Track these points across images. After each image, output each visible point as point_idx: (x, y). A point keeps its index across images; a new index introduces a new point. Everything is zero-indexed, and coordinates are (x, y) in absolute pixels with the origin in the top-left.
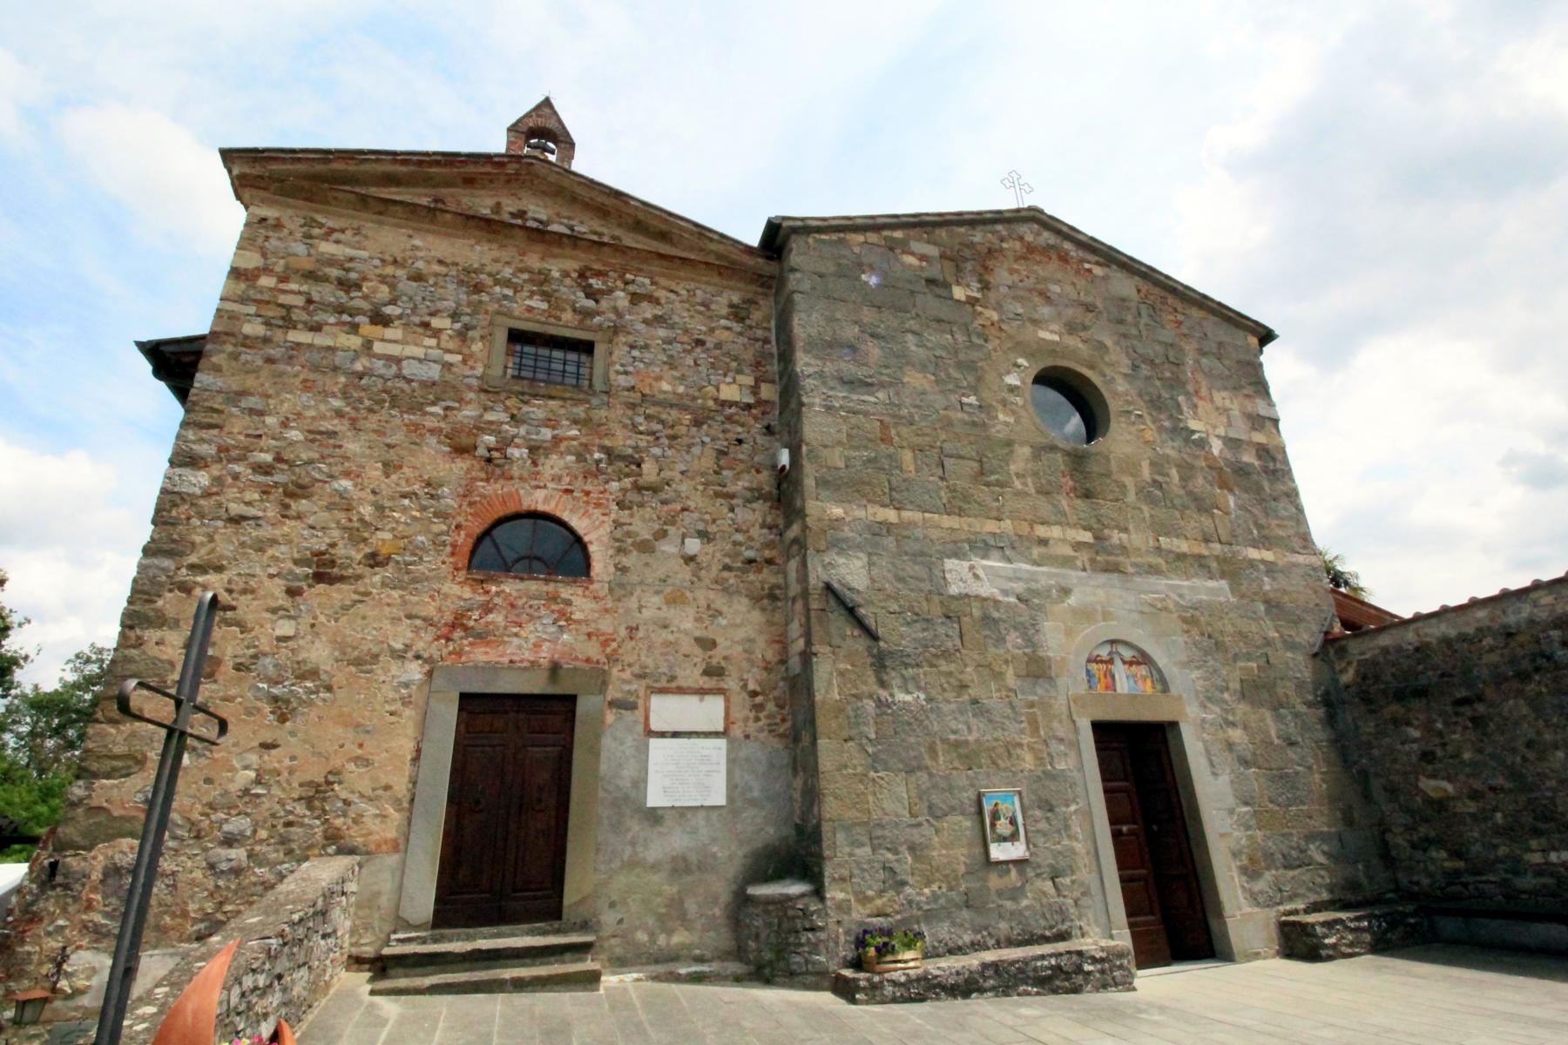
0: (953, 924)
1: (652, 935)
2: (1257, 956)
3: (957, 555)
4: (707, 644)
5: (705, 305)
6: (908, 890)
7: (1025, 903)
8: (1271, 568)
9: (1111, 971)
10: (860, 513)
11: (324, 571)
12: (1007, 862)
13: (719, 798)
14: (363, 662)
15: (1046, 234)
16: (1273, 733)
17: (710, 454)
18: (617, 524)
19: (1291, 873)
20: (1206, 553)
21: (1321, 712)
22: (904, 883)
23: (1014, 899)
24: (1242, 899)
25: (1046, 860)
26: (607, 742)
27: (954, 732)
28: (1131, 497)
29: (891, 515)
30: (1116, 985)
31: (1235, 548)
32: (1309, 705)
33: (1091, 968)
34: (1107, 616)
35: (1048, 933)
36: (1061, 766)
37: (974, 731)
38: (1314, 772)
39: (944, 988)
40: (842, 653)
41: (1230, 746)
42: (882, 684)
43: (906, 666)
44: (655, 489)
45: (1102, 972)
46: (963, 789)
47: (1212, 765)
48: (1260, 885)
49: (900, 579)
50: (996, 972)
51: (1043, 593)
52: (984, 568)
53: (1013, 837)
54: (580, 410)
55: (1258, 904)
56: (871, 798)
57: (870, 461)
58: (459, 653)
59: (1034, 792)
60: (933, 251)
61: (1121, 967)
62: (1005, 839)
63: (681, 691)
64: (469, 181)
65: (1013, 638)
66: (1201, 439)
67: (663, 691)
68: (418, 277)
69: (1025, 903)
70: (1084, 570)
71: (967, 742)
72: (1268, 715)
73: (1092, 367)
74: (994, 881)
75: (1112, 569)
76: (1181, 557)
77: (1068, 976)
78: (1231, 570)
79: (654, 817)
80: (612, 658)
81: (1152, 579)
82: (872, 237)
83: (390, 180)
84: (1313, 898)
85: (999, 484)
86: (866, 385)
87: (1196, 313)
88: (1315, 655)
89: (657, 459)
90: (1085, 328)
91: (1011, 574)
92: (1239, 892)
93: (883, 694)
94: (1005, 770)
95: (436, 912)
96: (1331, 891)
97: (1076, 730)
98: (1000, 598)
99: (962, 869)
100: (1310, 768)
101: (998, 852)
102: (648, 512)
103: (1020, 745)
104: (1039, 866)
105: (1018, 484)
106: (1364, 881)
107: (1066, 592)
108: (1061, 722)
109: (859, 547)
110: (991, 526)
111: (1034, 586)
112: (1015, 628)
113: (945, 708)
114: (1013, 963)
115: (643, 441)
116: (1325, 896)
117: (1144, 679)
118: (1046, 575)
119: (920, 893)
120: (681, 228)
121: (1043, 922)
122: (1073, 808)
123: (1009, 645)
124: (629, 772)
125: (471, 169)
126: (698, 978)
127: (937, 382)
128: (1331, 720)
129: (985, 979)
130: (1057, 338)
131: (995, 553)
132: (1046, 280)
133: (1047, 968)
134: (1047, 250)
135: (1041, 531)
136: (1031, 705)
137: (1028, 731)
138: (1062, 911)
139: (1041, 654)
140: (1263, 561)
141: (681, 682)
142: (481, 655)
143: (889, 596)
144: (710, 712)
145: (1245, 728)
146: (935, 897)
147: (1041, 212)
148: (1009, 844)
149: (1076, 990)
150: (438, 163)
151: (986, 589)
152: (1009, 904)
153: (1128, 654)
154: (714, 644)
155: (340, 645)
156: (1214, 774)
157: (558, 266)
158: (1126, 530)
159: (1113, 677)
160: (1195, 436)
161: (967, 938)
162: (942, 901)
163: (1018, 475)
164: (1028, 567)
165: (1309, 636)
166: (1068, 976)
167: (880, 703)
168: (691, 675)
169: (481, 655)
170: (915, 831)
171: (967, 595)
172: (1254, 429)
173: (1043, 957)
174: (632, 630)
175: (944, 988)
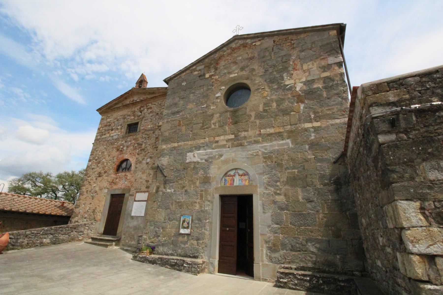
0: (168, 248)
1: (129, 241)
2: (265, 280)
3: (191, 151)
4: (147, 181)
5: (160, 105)
6: (160, 238)
7: (187, 246)
8: (316, 129)
9: (191, 268)
11: (100, 175)
12: (184, 234)
13: (143, 215)
14: (101, 189)
15: (240, 42)
16: (300, 198)
17: (154, 139)
18: (137, 158)
19: (294, 253)
21: (332, 187)
22: (159, 236)
23: (185, 244)
24: (265, 258)
25: (195, 235)
26: (128, 202)
27: (179, 199)
28: (253, 119)
29: (176, 145)
30: (192, 272)
31: (297, 125)
32: (325, 185)
33: (186, 265)
34: (234, 161)
35: (191, 255)
36: (207, 208)
37: (183, 198)
38: (320, 213)
39: (148, 261)
40: (158, 181)
41: (274, 202)
42: (165, 188)
43: (171, 183)
44: (144, 150)
45: (189, 267)
46: (178, 214)
47: (264, 208)
48: (277, 255)
50: (161, 260)
52: (197, 153)
53: (188, 228)
54: (135, 137)
55: (272, 262)
56: (156, 215)
57: (174, 132)
58: (112, 187)
59: (196, 215)
60: (202, 67)
61: (194, 267)
62: (185, 228)
63: (141, 192)
64: (126, 98)
65: (201, 172)
66: (291, 87)
67: (138, 192)
68: (118, 120)
69: (187, 246)
70: (229, 147)
71: (181, 202)
72: (299, 190)
73: (247, 79)
74: (180, 239)
75: (241, 145)
76: (270, 135)
78: (291, 134)
79: (132, 217)
80: (132, 186)
81: (255, 145)
82: (188, 72)
83: (116, 104)
84: (302, 265)
85: (207, 128)
86: (178, 112)
87: (302, 36)
88: (335, 163)
89: (145, 143)
90: (247, 66)
91: (204, 154)
92: (264, 256)
93: (164, 190)
94: (190, 209)
95: (104, 232)
96: (315, 264)
97: (214, 198)
98: (200, 161)
99: (173, 234)
100: (317, 211)
101: (182, 231)
102: (142, 155)
103: (196, 202)
104: (193, 237)
105: (213, 126)
106: (339, 264)
107: (221, 156)
108: (210, 195)
109: (167, 154)
110: (202, 141)
111: (211, 156)
112: (202, 169)
113: (178, 193)
114: (166, 259)
115: (143, 140)
116: (310, 265)
117: (246, 180)
118: (215, 152)
119: (162, 239)
120: (155, 90)
121: (190, 252)
122: (207, 221)
123: (199, 175)
124: (130, 209)
125: (125, 96)
126: (127, 250)
127: (196, 104)
128: (337, 190)
129: (158, 261)
130: (236, 75)
131: (202, 149)
132: (236, 57)
133: (174, 262)
134: (239, 48)
135: (217, 139)
136: (202, 191)
137: (199, 199)
138: (197, 250)
139: (208, 176)
140: (313, 127)
141: (142, 190)
142: (115, 187)
143: (171, 166)
144: (144, 196)
145: (285, 195)
146: (165, 241)
147: (237, 36)
148: (186, 229)
149: (180, 270)
150: (120, 98)
151: (196, 159)
152: (183, 246)
153: (241, 172)
154: (149, 181)
155: (100, 187)
156: (264, 212)
157: (136, 109)
158: (247, 131)
159: (234, 181)
160: (288, 87)
161: (170, 252)
162: (167, 242)
163: (213, 124)
164: (210, 150)
165: (332, 155)
168: (144, 189)
169: (115, 187)
170: (164, 224)
171: (191, 162)
173: (173, 259)
174: (136, 180)
175: (148, 261)
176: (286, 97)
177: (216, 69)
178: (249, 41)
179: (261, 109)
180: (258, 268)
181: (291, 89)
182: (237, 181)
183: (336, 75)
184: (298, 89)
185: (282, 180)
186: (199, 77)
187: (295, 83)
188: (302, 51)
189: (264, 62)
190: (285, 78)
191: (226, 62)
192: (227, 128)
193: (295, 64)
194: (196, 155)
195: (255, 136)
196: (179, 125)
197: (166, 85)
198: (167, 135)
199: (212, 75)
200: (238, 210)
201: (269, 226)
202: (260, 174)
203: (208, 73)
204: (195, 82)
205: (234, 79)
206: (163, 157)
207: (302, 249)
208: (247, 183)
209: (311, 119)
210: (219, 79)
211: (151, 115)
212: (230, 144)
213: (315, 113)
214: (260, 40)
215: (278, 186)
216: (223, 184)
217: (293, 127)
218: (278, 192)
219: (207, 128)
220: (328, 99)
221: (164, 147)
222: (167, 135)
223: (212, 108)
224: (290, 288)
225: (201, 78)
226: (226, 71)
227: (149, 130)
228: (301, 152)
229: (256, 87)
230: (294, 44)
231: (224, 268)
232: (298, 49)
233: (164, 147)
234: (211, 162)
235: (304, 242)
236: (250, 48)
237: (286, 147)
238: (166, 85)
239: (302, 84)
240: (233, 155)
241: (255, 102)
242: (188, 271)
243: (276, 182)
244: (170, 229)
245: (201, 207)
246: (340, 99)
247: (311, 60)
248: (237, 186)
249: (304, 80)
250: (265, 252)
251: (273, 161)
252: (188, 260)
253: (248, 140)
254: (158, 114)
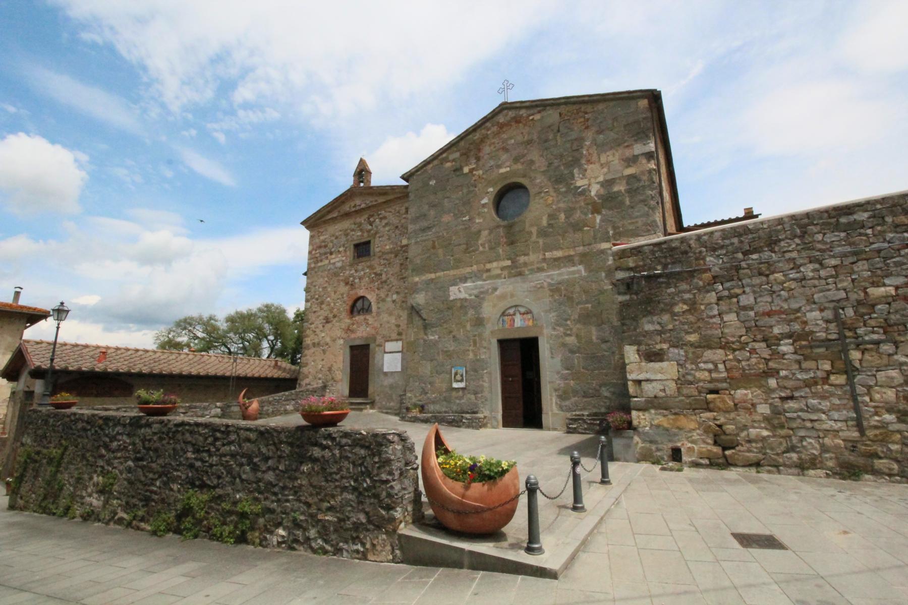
2: (555, 429)
4: (398, 326)
5: (399, 212)
10: (424, 278)
11: (327, 321)
13: (399, 369)
14: (334, 340)
15: (510, 113)
16: (594, 338)
20: (572, 253)
28: (534, 237)
29: (433, 276)
36: (483, 357)
37: (451, 346)
41: (564, 345)
42: (426, 334)
44: (385, 282)
48: (567, 403)
49: (434, 298)
51: (486, 292)
53: (461, 381)
54: (368, 264)
60: (457, 155)
63: (392, 341)
64: (343, 202)
65: (471, 312)
66: (584, 190)
68: (337, 238)
73: (524, 176)
74: (454, 394)
75: (520, 274)
76: (557, 259)
77: (457, 422)
78: (584, 258)
79: (386, 374)
80: (377, 333)
81: (538, 274)
82: (436, 162)
84: (595, 410)
85: (473, 251)
86: (429, 228)
87: (601, 106)
90: (524, 156)
92: (554, 405)
101: (455, 385)
102: (384, 290)
105: (481, 249)
107: (495, 289)
109: (422, 290)
110: (468, 270)
115: (381, 268)
117: (529, 320)
118: (487, 284)
126: (387, 413)
130: (508, 169)
132: (507, 140)
135: (488, 266)
136: (475, 336)
138: (476, 405)
142: (353, 336)
144: (398, 346)
145: (577, 336)
146: (435, 398)
147: (506, 103)
149: (459, 427)
151: (463, 295)
152: (458, 401)
153: (522, 310)
155: (331, 337)
156: (552, 357)
157: (362, 219)
166: (457, 422)
167: (425, 341)
168: (394, 336)
169: (353, 336)
172: (629, 166)
176: (577, 206)
177: (478, 159)
178: (523, 112)
179: (544, 222)
180: (547, 419)
181: (583, 193)
182: (518, 322)
183: (643, 173)
184: (593, 193)
185: (572, 318)
186: (454, 171)
187: (589, 185)
188: (600, 132)
189: (546, 149)
190: (576, 175)
191: (492, 147)
192: (501, 251)
193: (590, 154)
194: (462, 289)
195: (538, 262)
196: (434, 247)
197: (405, 183)
198: (418, 262)
199: (473, 169)
200: (521, 356)
201: (558, 373)
202: (546, 312)
203: (467, 165)
204: (448, 180)
205: (505, 176)
206: (418, 293)
207: (597, 395)
208: (530, 323)
209: (609, 237)
210: (484, 176)
211: (387, 229)
212: (506, 273)
213: (614, 228)
214: (539, 112)
215: (567, 325)
216: (501, 325)
217: (586, 248)
218: (569, 332)
219: (473, 251)
220: (632, 207)
221: (417, 279)
222: (418, 262)
223: (477, 221)
224: (579, 433)
225: (458, 173)
226: (492, 163)
227: (388, 253)
228: (595, 282)
229: (537, 189)
230: (588, 120)
231: (509, 421)
232: (594, 129)
233: (417, 279)
234: (483, 299)
235: (598, 387)
236: (525, 125)
237: (577, 275)
238: (405, 183)
239: (599, 186)
240: (511, 288)
241: (538, 211)
242: (468, 427)
243: (566, 320)
244: (440, 383)
245: (475, 355)
246: (646, 209)
247: (611, 148)
248: (518, 328)
249: (601, 179)
250: (554, 400)
251: (562, 294)
252: (468, 416)
253: (530, 268)
254: (397, 227)
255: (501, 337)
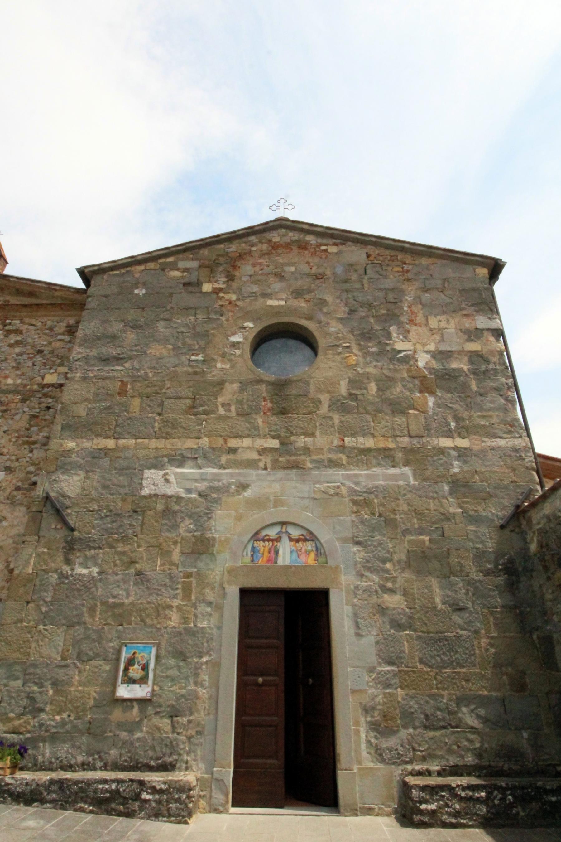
0: (73, 746)
2: (368, 811)
3: (157, 465)
5: (51, 329)
6: (43, 716)
7: (138, 735)
8: (463, 454)
9: (168, 802)
10: (87, 444)
15: (291, 234)
16: (438, 600)
17: (26, 417)
19: (431, 734)
20: (391, 445)
21: (501, 580)
22: (42, 710)
24: (364, 754)
27: (114, 597)
28: (324, 409)
29: (110, 443)
30: (170, 816)
31: (424, 440)
32: (487, 573)
33: (148, 797)
34: (278, 503)
35: (152, 763)
36: (205, 624)
37: (129, 595)
38: (482, 636)
40: (43, 540)
41: (382, 610)
42: (68, 562)
45: (159, 802)
46: (111, 641)
47: (357, 626)
49: (105, 487)
50: (61, 788)
51: (225, 490)
52: (176, 474)
53: (143, 680)
55: (383, 761)
56: (33, 645)
57: (106, 408)
60: (194, 264)
61: (178, 800)
62: (134, 682)
66: (407, 356)
69: (138, 735)
70: (266, 469)
71: (122, 604)
72: (434, 583)
74: (117, 714)
75: (296, 466)
77: (125, 801)
78: (414, 457)
81: (330, 471)
82: (151, 265)
84: (453, 760)
85: (205, 413)
86: (118, 359)
87: (424, 261)
88: (502, 527)
90: (310, 291)
91: (197, 477)
92: (363, 746)
93: (66, 569)
94: (152, 626)
96: (480, 756)
97: (224, 595)
98: (183, 495)
99: (92, 702)
100: (476, 632)
101: (124, 691)
103: (170, 607)
104: (160, 706)
105: (222, 411)
106: (529, 751)
107: (244, 487)
108: (213, 589)
109: (80, 467)
110: (190, 443)
111: (216, 484)
112: (190, 517)
113: (111, 578)
114: (77, 782)
116: (470, 759)
117: (308, 553)
119: (51, 718)
121: (150, 753)
122: (204, 660)
123: (181, 531)
127: (174, 349)
128: (512, 586)
130: (282, 303)
131: (190, 463)
132: (283, 265)
133: (107, 791)
134: (288, 246)
135: (233, 443)
136: (189, 575)
138: (173, 747)
139: (208, 535)
140: (455, 448)
143: (93, 499)
145: (405, 594)
146: (63, 723)
147: (287, 220)
149: (129, 814)
151: (172, 489)
152: (124, 735)
153: (295, 533)
156: (358, 635)
158: (312, 435)
159: (277, 553)
160: (401, 355)
161: (80, 759)
162: (68, 727)
163: (223, 405)
164: (215, 471)
165: (497, 510)
166: (125, 801)
167: (62, 576)
171: (156, 495)
172: (470, 340)
173: (105, 781)
176: (398, 376)
177: (231, 278)
178: (310, 238)
179: (343, 389)
180: (347, 783)
181: (406, 360)
182: (286, 555)
183: (492, 352)
184: (421, 364)
185: (396, 557)
186: (185, 284)
187: (415, 351)
188: (426, 290)
189: (347, 291)
190: (395, 335)
191: (257, 268)
192: (260, 421)
193: (413, 313)
194: (172, 478)
195: (330, 451)
196: (122, 392)
197: (80, 284)
198: (83, 413)
199: (221, 290)
200: (289, 630)
201: (371, 670)
202: (345, 540)
203: (209, 281)
204: (171, 295)
205: (276, 311)
206: (66, 471)
207: (453, 724)
208: (311, 560)
209: (450, 430)
210: (238, 303)
211: (17, 350)
212: (268, 459)
213: (457, 419)
214: (335, 244)
215: (387, 571)
216: (248, 559)
217: (415, 441)
218: (389, 585)
219: (205, 413)
220: (481, 395)
221: (71, 444)
222: (83, 413)
223: (219, 365)
224: (445, 825)
225: (190, 289)
226: (255, 288)
227: (9, 392)
228: (434, 498)
229: (331, 341)
230: (408, 271)
231: (247, 792)
232: (417, 284)
233: (71, 444)
234: (217, 501)
235: (453, 706)
236: (314, 254)
237: (401, 483)
238: (80, 284)
239: (429, 356)
240: (277, 487)
241: (329, 371)
242: (156, 815)
243: (384, 561)
244: (83, 685)
245: (186, 620)
246: (502, 401)
247: (444, 313)
248: (287, 568)
249: (432, 347)
250: (363, 735)
251: (375, 513)
252: (156, 778)
253: (314, 457)
254: (40, 352)
255: (241, 586)
